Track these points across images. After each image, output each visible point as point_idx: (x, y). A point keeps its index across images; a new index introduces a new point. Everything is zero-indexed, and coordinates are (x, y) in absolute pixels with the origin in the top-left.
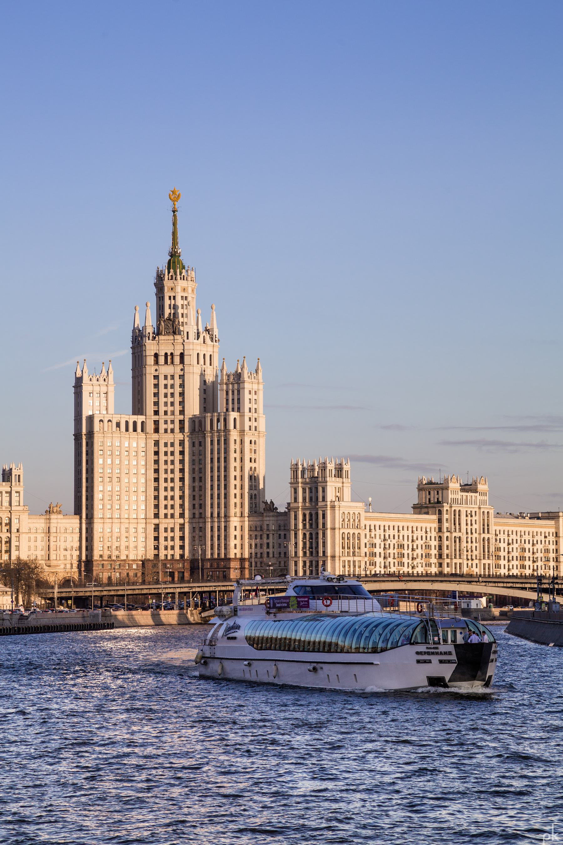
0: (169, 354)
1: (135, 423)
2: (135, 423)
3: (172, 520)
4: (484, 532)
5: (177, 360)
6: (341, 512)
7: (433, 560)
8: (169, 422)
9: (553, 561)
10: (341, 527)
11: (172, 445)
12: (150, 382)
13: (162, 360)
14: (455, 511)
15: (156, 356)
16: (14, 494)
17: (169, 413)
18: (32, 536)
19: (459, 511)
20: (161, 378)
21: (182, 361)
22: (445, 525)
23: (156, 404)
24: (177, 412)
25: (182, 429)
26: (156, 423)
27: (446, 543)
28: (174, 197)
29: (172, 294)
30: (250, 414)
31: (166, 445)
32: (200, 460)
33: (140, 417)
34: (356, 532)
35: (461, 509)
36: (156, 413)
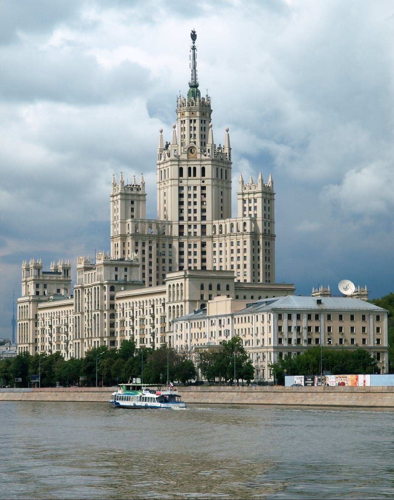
0: (192, 167)
8: (192, 226)
11: (195, 246)
15: (181, 170)
20: (185, 188)
21: (203, 174)
23: (181, 211)
24: (199, 218)
25: (203, 232)
28: (194, 36)
29: (193, 119)
30: (265, 220)
31: (189, 246)
32: (221, 259)
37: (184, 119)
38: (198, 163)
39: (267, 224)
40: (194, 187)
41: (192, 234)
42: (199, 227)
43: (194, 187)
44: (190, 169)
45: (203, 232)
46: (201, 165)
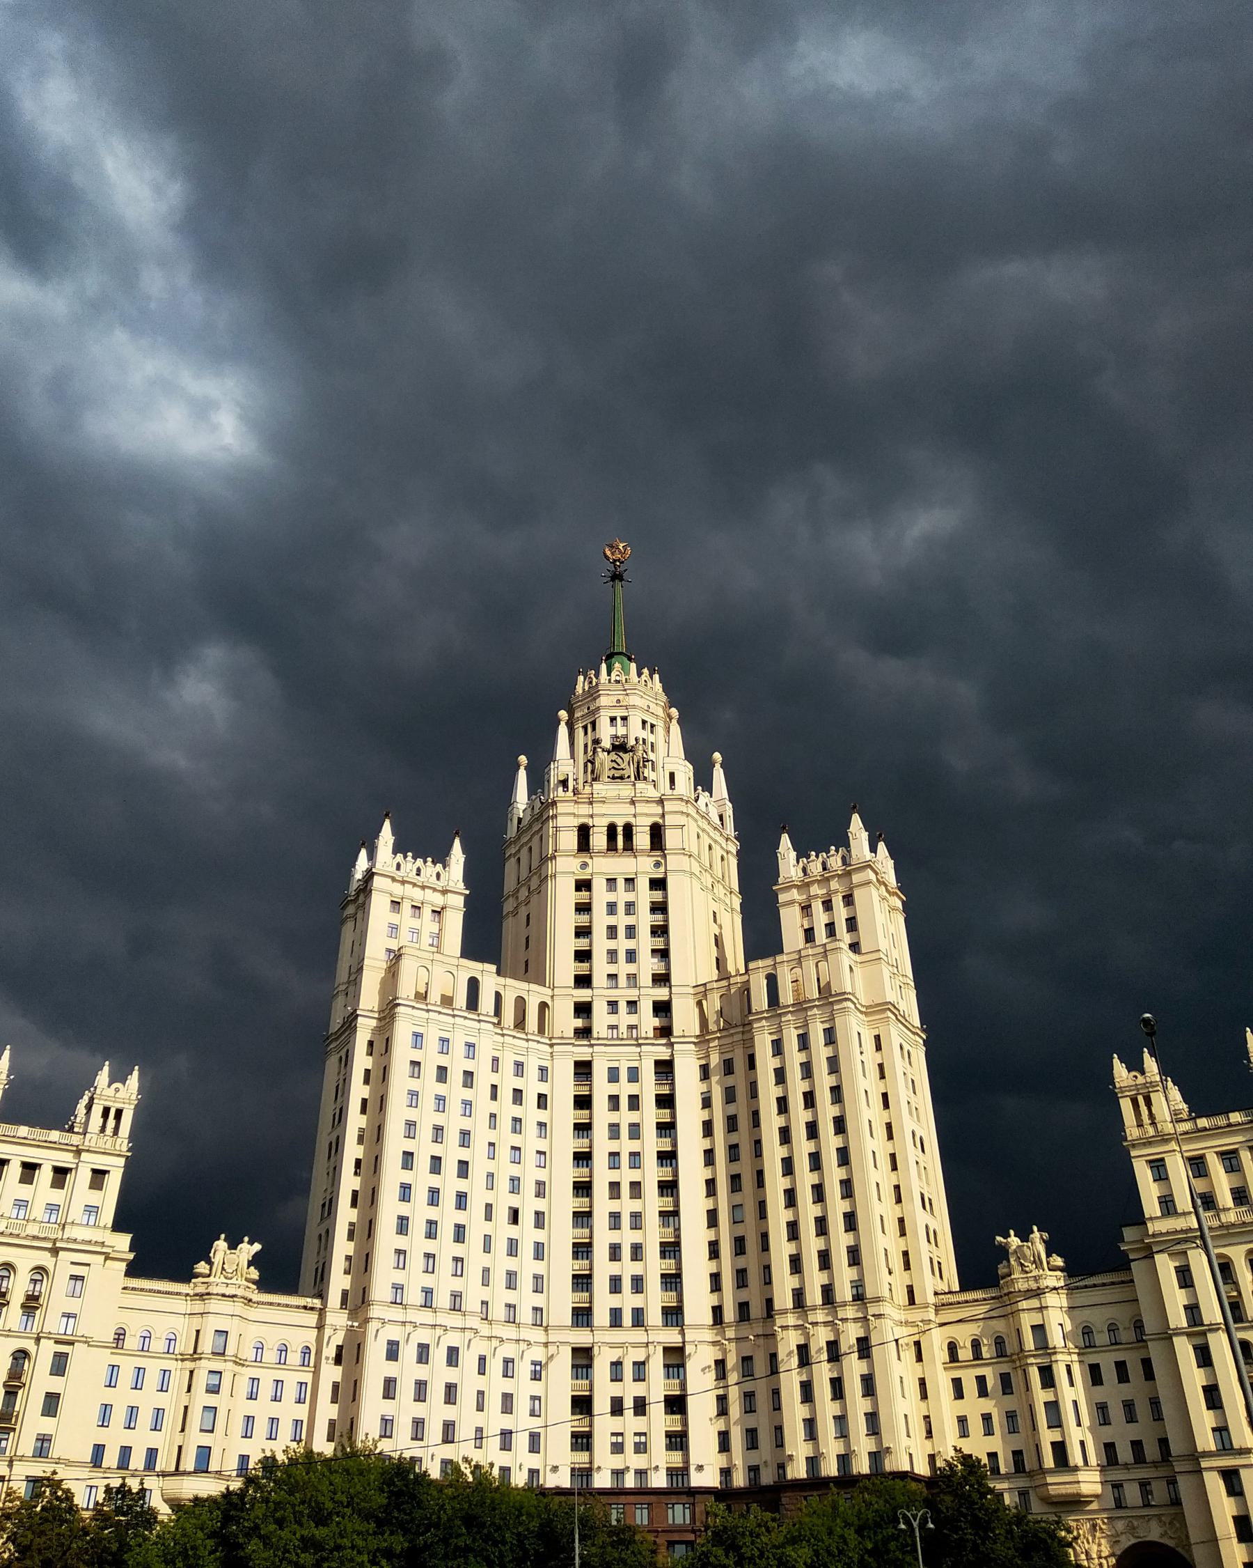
0: (620, 822)
1: (521, 1003)
2: (521, 1003)
5: (642, 839)
8: (623, 1006)
11: (634, 1075)
12: (563, 896)
13: (599, 840)
15: (584, 832)
17: (622, 980)
18: (127, 1366)
20: (599, 885)
23: (583, 956)
24: (646, 979)
26: (583, 1009)
31: (613, 1075)
33: (533, 987)
36: (583, 981)
37: (593, 719)
38: (641, 808)
40: (626, 880)
42: (646, 1007)
43: (626, 880)
44: (612, 829)
45: (665, 1032)
46: (647, 815)
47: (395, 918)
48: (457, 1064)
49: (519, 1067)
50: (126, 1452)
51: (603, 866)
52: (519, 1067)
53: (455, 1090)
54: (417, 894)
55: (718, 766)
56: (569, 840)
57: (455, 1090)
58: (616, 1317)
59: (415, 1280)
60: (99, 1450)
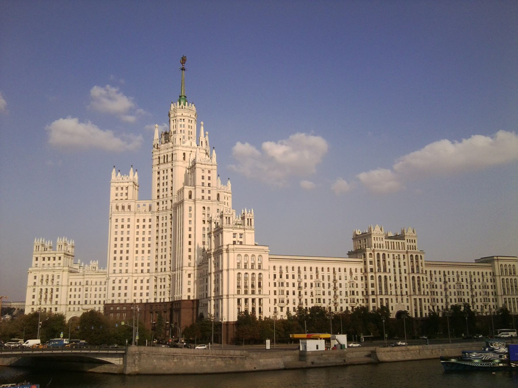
0: (166, 155)
3: (164, 273)
4: (413, 272)
5: (170, 159)
6: (236, 254)
7: (360, 297)
8: (165, 202)
9: (492, 295)
10: (236, 267)
14: (378, 254)
16: (57, 258)
17: (165, 196)
19: (384, 254)
20: (161, 172)
22: (369, 266)
26: (158, 204)
27: (370, 282)
34: (257, 273)
35: (386, 254)
39: (206, 191)
41: (165, 209)
47: (117, 192)
48: (126, 224)
49: (144, 220)
50: (75, 302)
51: (162, 167)
52: (144, 220)
53: (126, 229)
54: (122, 184)
55: (202, 126)
56: (156, 162)
57: (126, 229)
58: (161, 271)
59: (118, 268)
60: (70, 302)
